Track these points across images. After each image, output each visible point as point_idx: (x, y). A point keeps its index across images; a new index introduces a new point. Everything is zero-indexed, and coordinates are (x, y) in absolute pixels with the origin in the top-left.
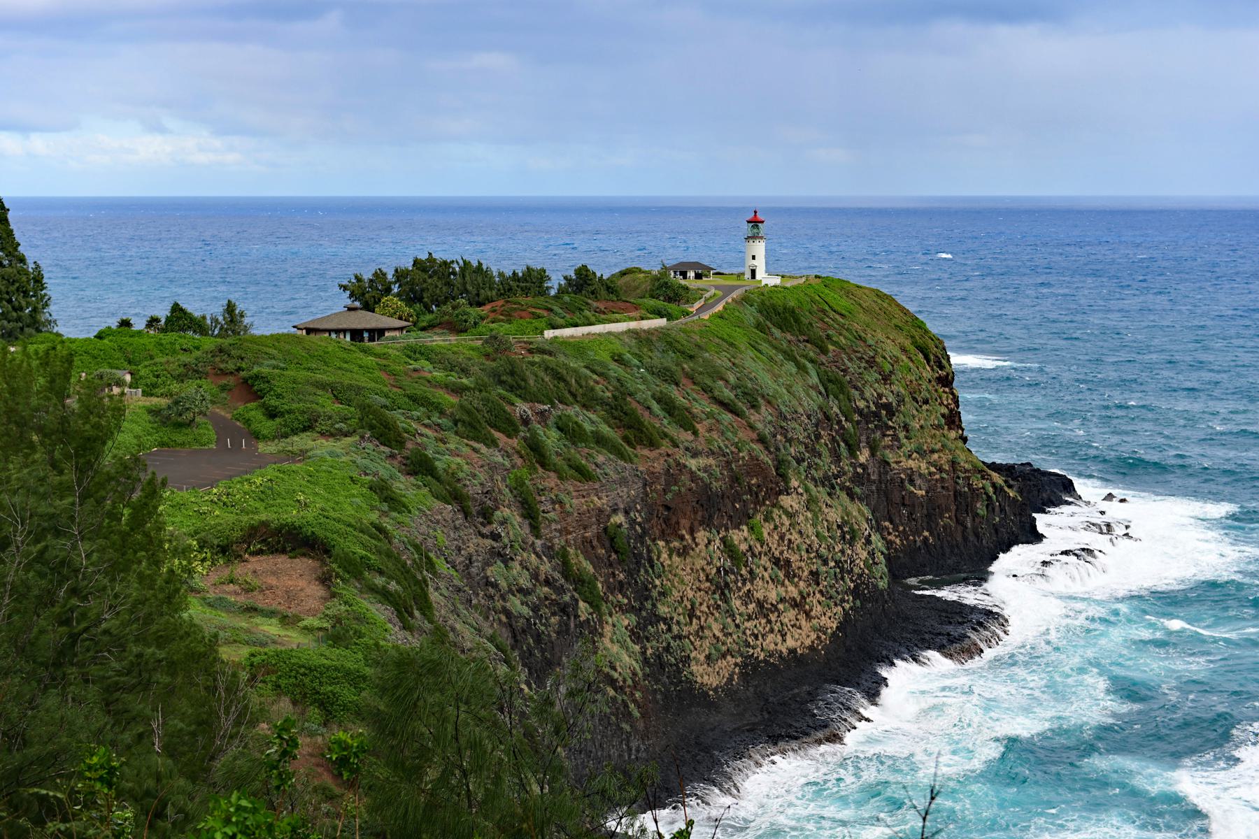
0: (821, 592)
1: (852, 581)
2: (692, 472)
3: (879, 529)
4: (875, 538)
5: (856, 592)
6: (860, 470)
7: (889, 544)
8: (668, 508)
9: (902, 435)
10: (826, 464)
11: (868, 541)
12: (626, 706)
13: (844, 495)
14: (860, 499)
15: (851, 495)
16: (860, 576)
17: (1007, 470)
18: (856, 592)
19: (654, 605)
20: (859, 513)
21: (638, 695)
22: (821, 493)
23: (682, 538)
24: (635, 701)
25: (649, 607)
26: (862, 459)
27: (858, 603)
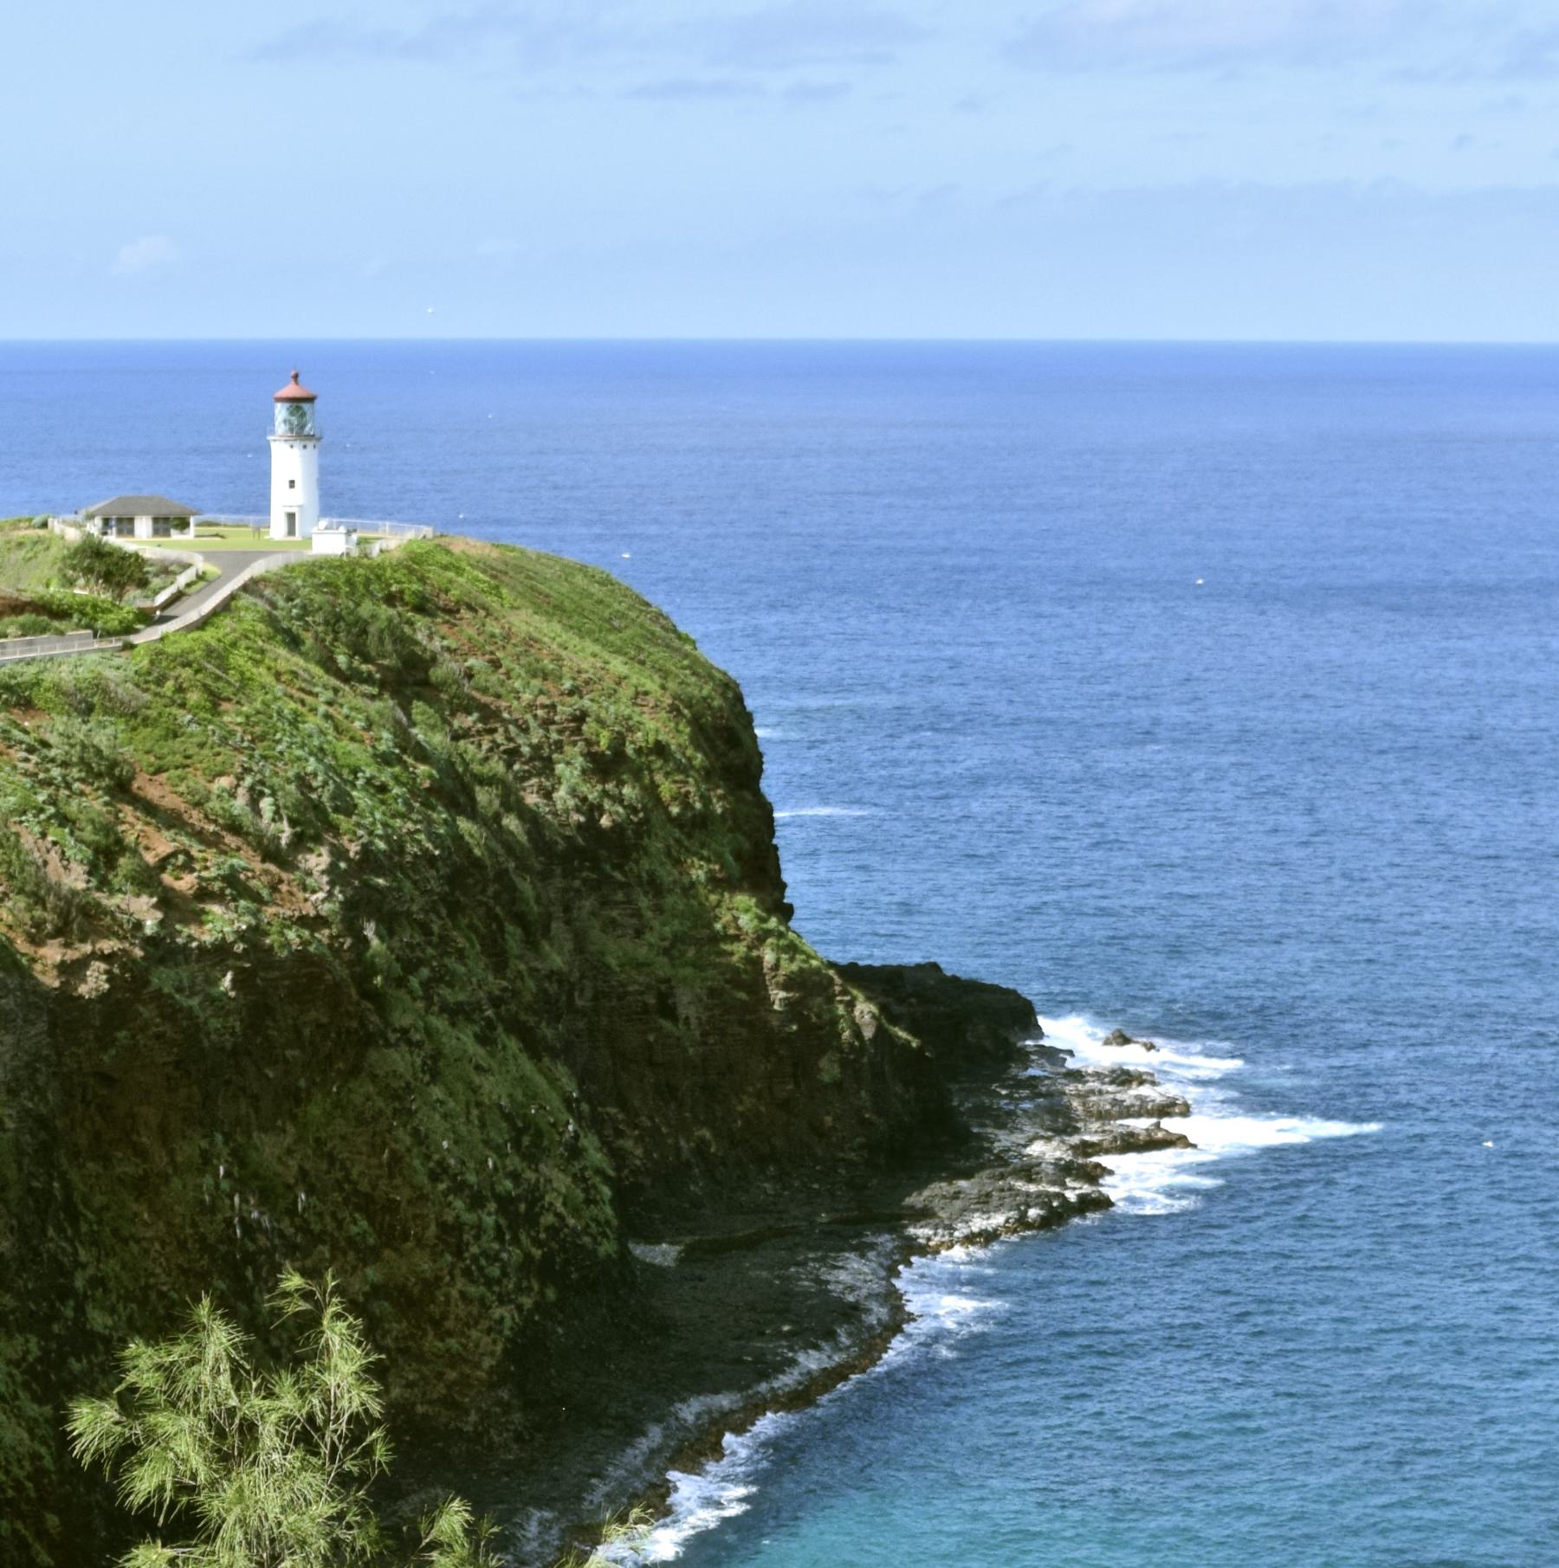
0: (467, 1273)
1: (538, 1243)
2: (158, 995)
3: (596, 1123)
4: (590, 1142)
5: (545, 1270)
6: (552, 988)
7: (617, 1155)
8: (106, 1079)
9: (644, 902)
10: (475, 977)
11: (575, 1151)
12: (23, 1545)
13: (513, 1044)
14: (555, 1056)
15: (534, 1047)
16: (553, 1231)
17: (885, 983)
18: (545, 1270)
19: (80, 1310)
20: (552, 1090)
21: (52, 1520)
22: (463, 1040)
23: (141, 1153)
24: (42, 1534)
25: (69, 1313)
26: (557, 961)
27: (551, 1294)
